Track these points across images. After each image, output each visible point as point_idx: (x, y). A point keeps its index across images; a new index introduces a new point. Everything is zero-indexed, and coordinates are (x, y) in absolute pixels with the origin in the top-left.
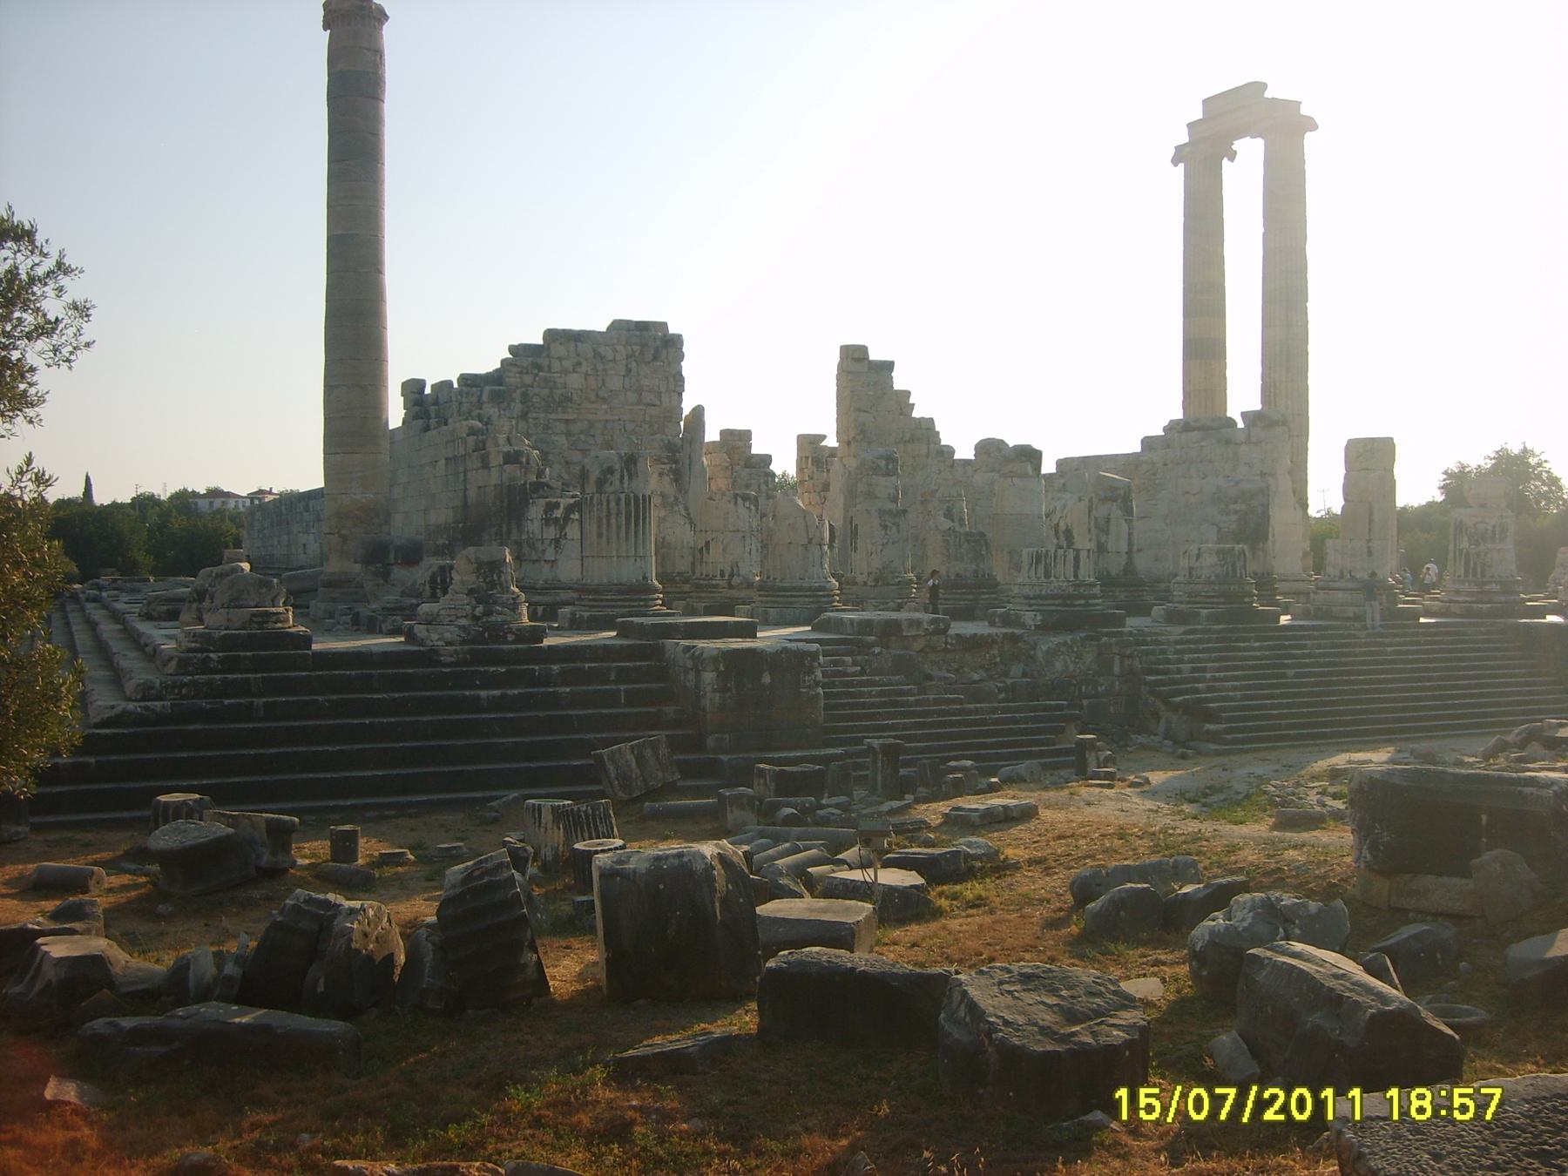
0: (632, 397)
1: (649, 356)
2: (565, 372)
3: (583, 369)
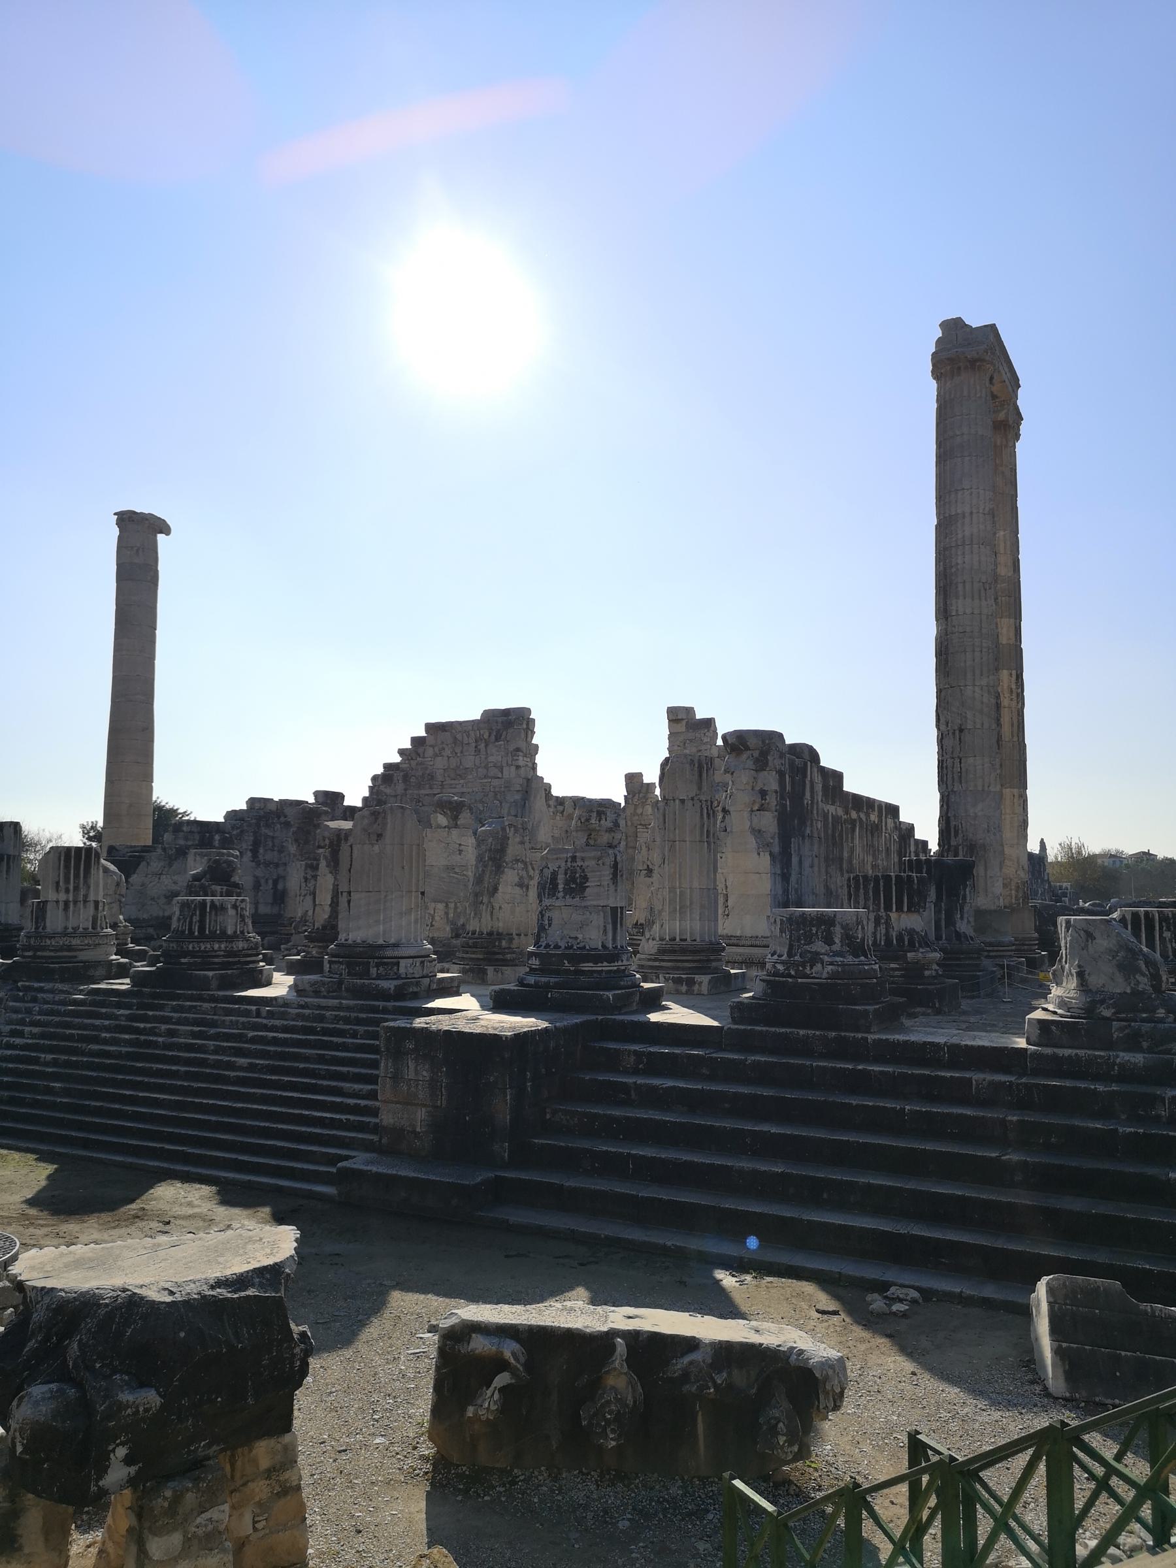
0: (482, 771)
1: (493, 737)
2: (436, 755)
3: (448, 752)
